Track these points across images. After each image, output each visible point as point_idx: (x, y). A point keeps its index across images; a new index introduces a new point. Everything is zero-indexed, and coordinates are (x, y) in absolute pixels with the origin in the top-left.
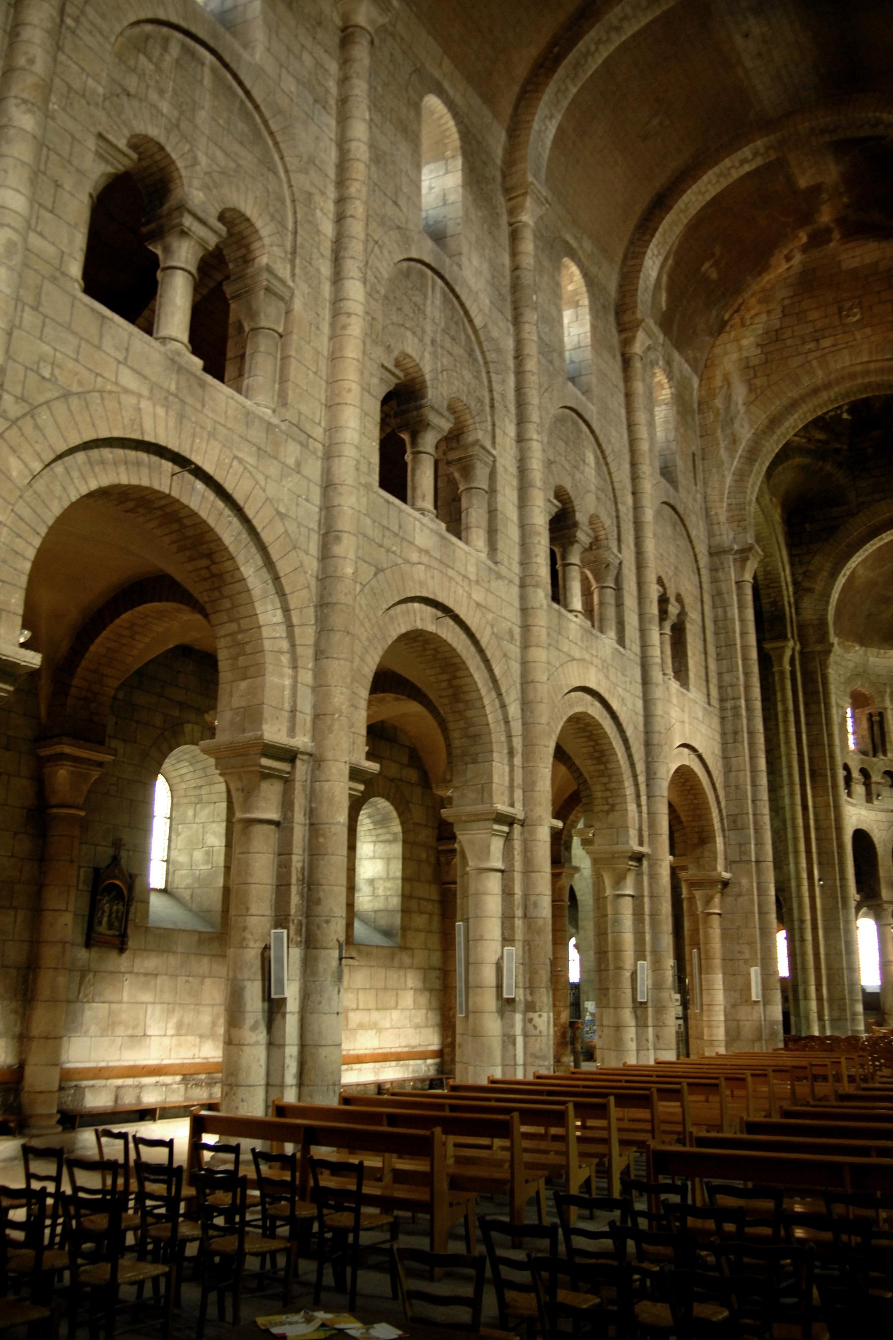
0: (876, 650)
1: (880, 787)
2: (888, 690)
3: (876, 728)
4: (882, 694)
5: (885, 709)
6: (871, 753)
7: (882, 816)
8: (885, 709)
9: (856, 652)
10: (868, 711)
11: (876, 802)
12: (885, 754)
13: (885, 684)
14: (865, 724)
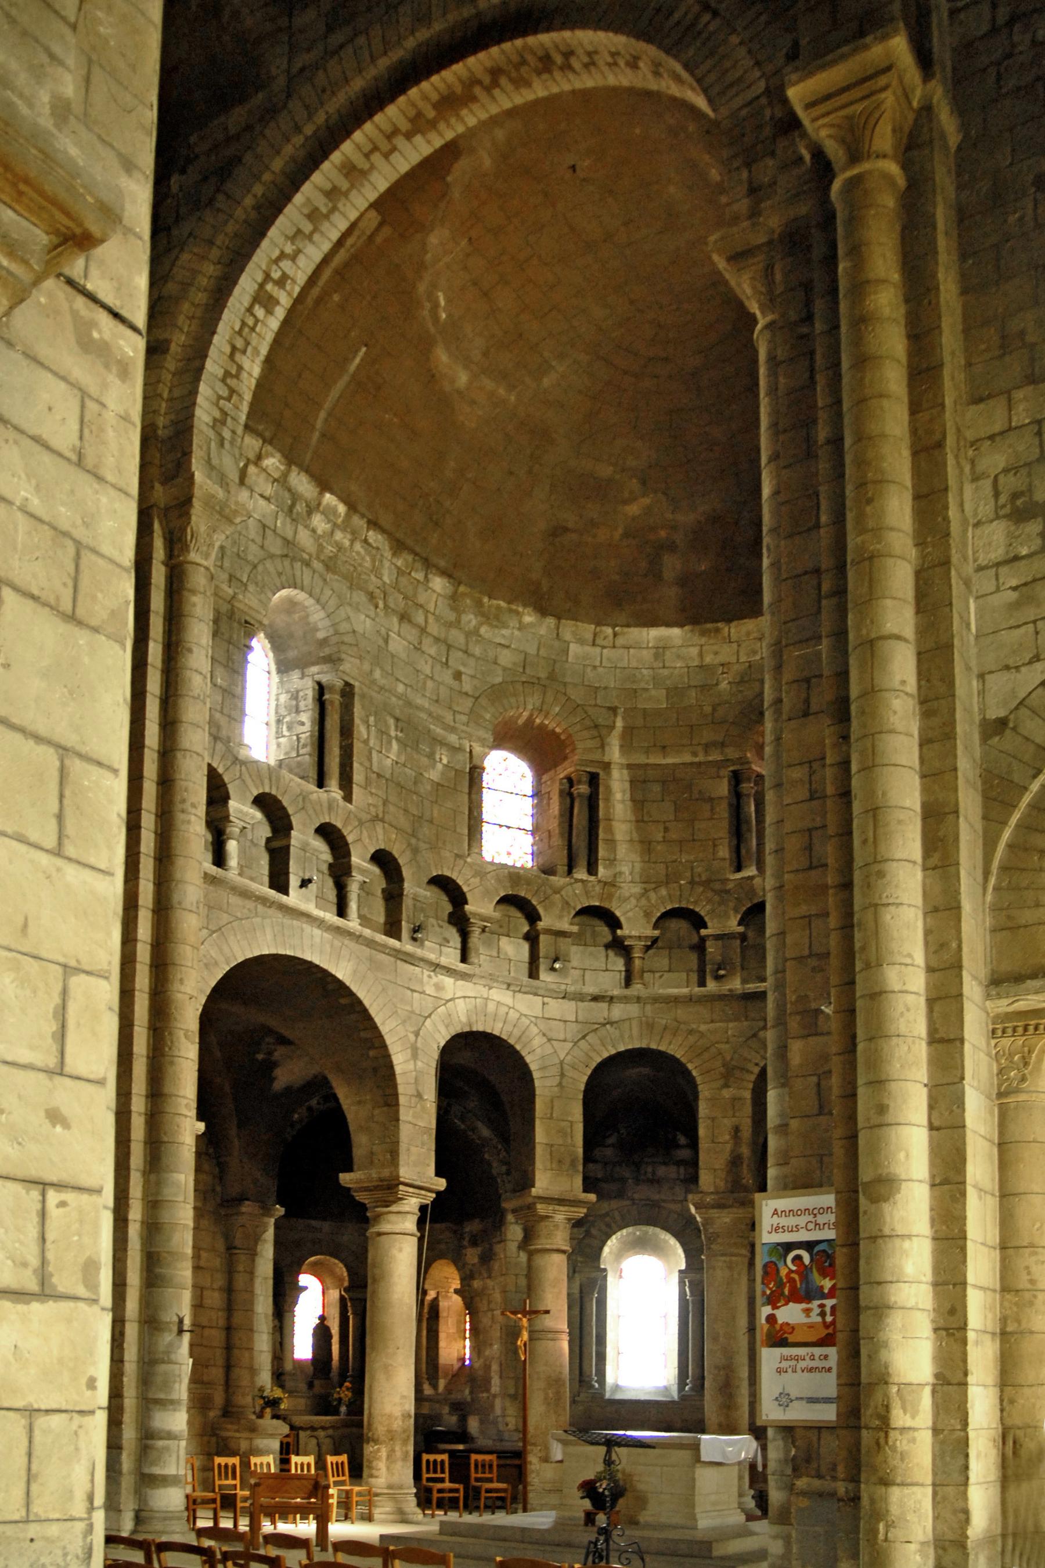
0: (587, 630)
9: (521, 627)
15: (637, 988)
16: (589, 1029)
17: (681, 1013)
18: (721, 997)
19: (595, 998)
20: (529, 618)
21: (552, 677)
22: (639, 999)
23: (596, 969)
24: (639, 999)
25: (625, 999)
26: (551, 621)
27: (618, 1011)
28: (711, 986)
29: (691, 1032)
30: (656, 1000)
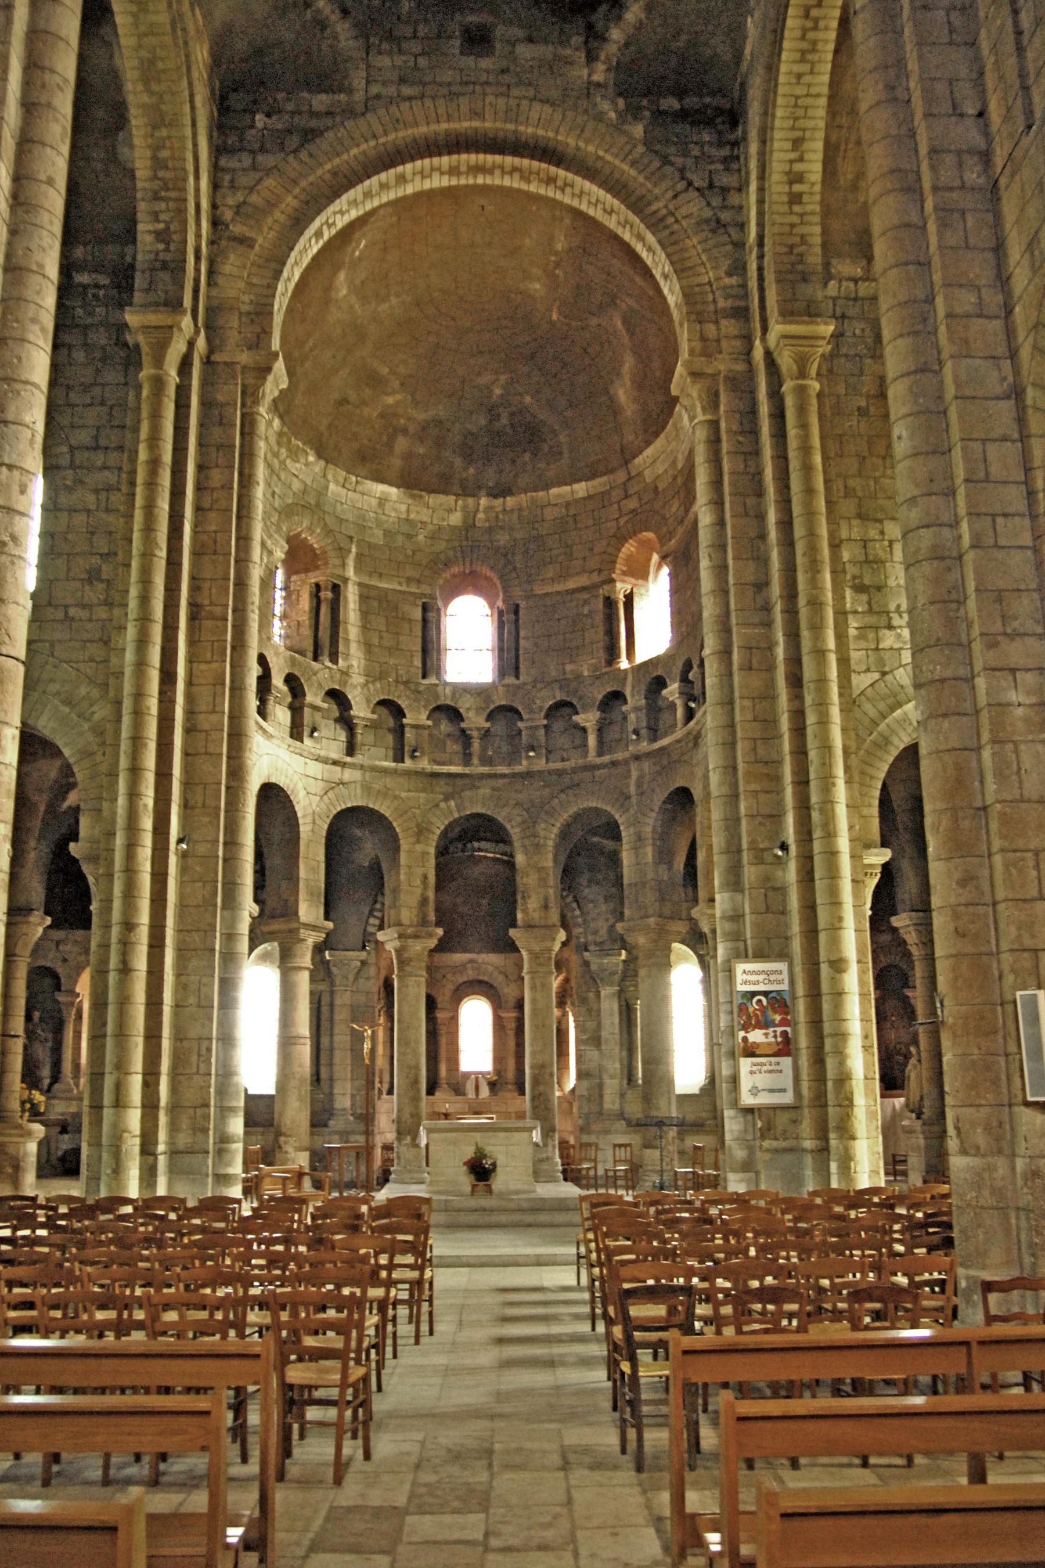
1: (318, 716)
2: (354, 550)
3: (324, 610)
4: (342, 552)
5: (346, 580)
6: (310, 654)
7: (316, 769)
8: (346, 580)
9: (307, 464)
10: (313, 578)
11: (307, 741)
12: (334, 658)
13: (351, 538)
14: (305, 603)
15: (358, 759)
16: (333, 786)
17: (389, 781)
18: (416, 773)
19: (335, 763)
20: (311, 459)
21: (318, 505)
22: (362, 767)
23: (330, 741)
24: (362, 767)
25: (353, 766)
26: (322, 463)
27: (348, 775)
28: (408, 763)
29: (396, 797)
30: (374, 769)
